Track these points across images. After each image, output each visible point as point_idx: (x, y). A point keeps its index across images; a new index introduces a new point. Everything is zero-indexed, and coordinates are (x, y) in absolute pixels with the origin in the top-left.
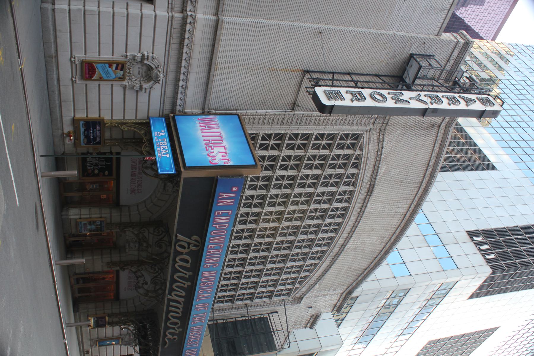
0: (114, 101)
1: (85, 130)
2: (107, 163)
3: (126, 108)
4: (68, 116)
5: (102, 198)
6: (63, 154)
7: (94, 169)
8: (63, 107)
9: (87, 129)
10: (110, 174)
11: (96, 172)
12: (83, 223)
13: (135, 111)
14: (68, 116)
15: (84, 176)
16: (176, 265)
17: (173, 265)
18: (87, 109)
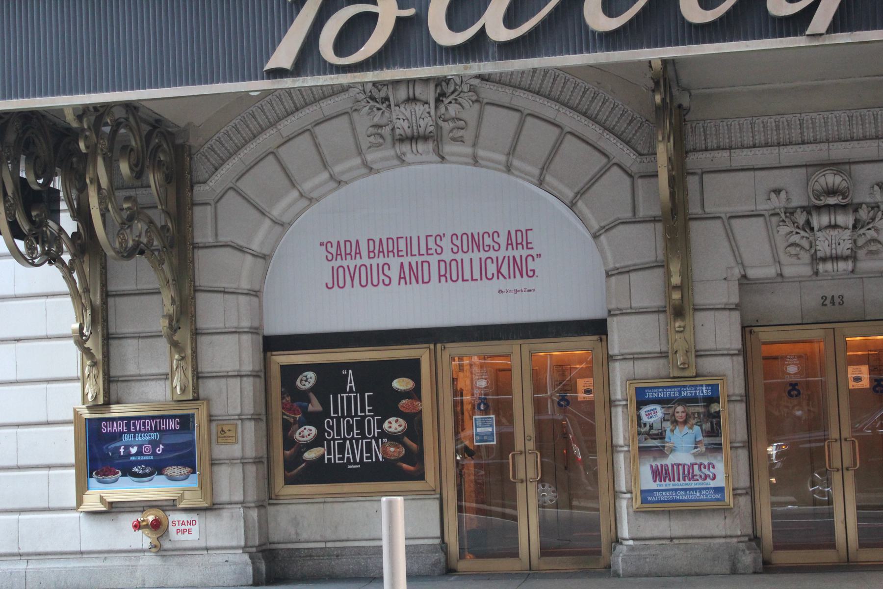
0: (12, 377)
1: (127, 471)
2: (351, 384)
3: (43, 333)
4: (75, 531)
5: (865, 383)
6: (245, 548)
7: (383, 434)
8: (41, 549)
9: (127, 468)
10: (411, 368)
11: (394, 425)
12: (648, 482)
13: (50, 300)
14: (75, 531)
15: (420, 476)
16: (499, 33)
17: (509, 49)
18: (49, 467)
